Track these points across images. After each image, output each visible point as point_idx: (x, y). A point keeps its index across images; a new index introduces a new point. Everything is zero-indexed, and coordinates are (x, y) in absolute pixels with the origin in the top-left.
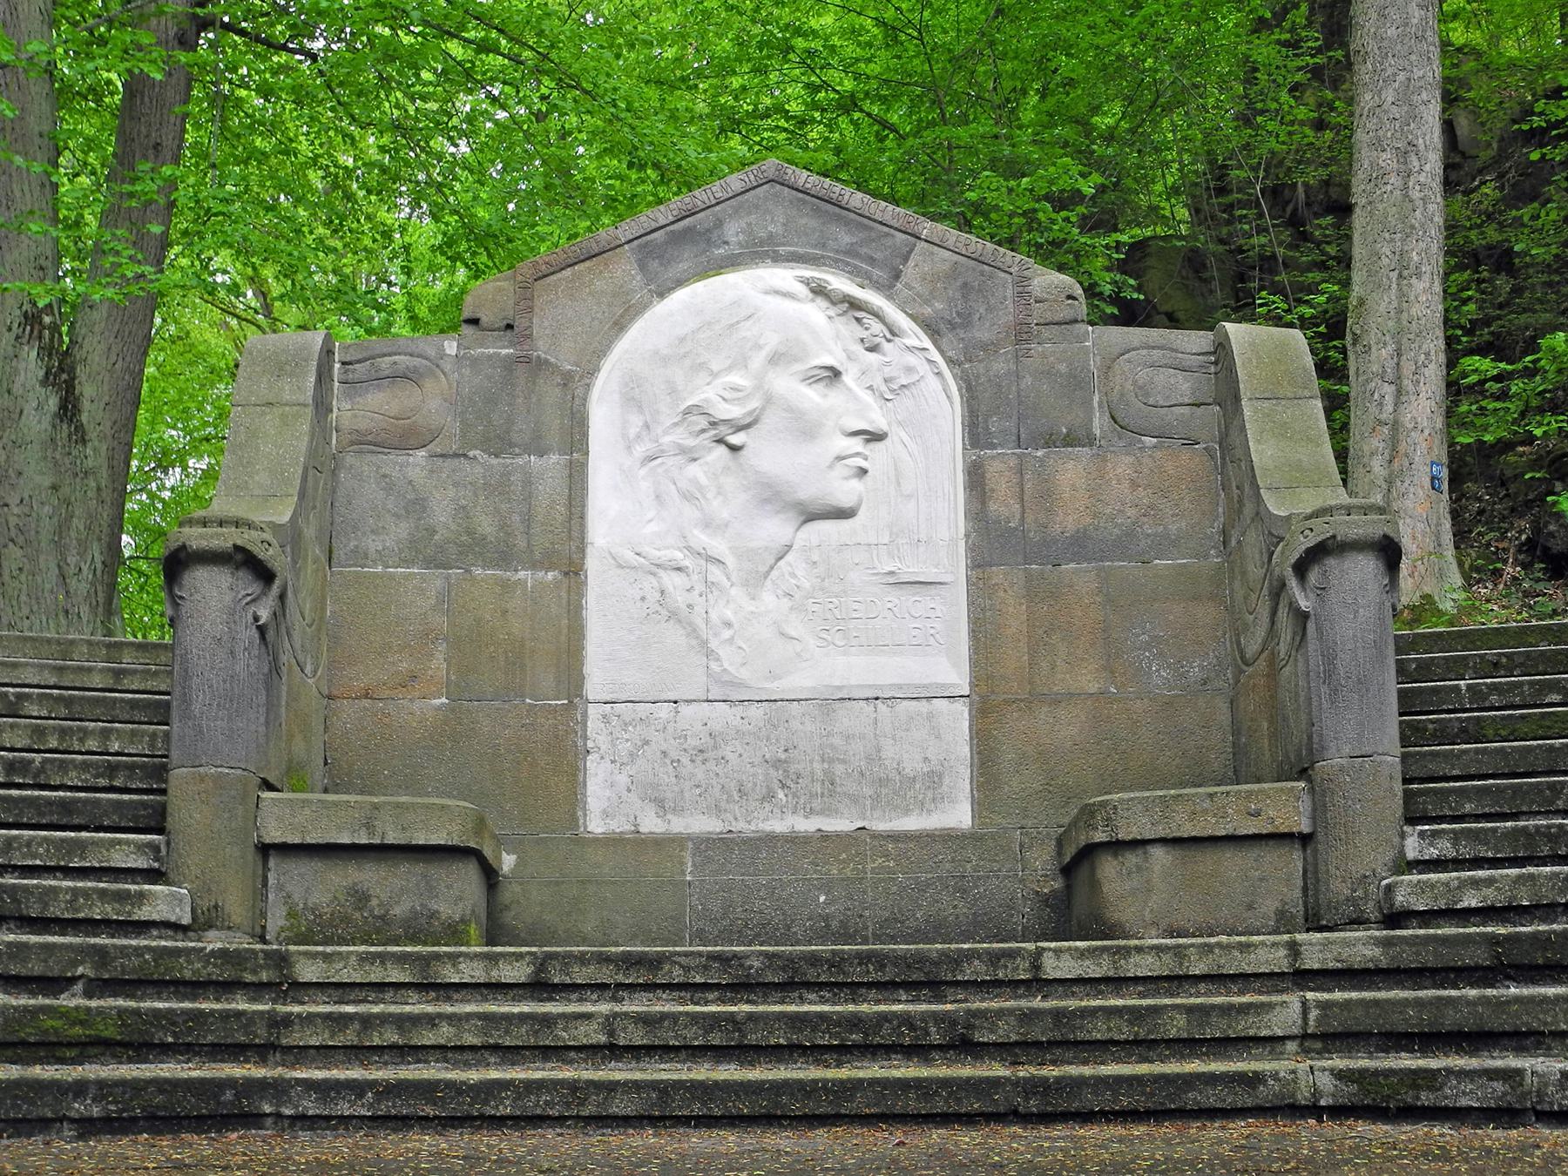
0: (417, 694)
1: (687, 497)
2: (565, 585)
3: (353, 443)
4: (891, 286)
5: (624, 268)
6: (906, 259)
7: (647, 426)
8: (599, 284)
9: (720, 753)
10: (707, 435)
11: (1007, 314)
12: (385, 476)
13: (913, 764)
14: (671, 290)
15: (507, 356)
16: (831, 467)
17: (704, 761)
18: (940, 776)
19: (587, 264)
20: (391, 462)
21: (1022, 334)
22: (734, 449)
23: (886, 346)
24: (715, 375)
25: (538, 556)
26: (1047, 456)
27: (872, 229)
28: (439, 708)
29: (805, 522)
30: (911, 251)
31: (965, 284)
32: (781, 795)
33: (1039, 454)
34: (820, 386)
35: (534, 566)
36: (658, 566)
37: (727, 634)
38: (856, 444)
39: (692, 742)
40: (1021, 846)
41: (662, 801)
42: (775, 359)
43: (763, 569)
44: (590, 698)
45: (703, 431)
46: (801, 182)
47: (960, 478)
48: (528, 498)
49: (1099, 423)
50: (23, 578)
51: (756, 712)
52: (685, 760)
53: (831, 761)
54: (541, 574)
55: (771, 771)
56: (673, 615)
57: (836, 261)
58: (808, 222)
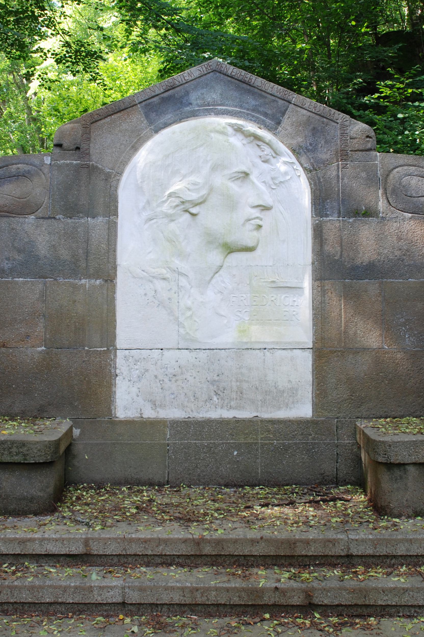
0: (29, 345)
4: (276, 129)
6: (283, 114)
7: (148, 202)
8: (125, 126)
9: (185, 377)
10: (177, 208)
12: (13, 229)
13: (282, 383)
15: (77, 164)
16: (244, 225)
17: (176, 381)
18: (297, 390)
19: (119, 115)
22: (193, 215)
23: (273, 160)
24: (184, 176)
25: (91, 271)
26: (354, 221)
27: (266, 97)
28: (40, 352)
29: (229, 253)
30: (287, 109)
31: (314, 128)
32: (215, 398)
33: (351, 220)
34: (238, 182)
35: (89, 277)
36: (154, 277)
37: (189, 313)
38: (256, 213)
39: (170, 371)
40: (337, 427)
41: (155, 401)
42: (215, 168)
43: (208, 278)
44: (118, 347)
46: (229, 72)
47: (310, 233)
48: (87, 241)
51: (203, 355)
52: (166, 380)
53: (241, 381)
54: (93, 281)
55: (212, 387)
56: (161, 304)
57: (248, 114)
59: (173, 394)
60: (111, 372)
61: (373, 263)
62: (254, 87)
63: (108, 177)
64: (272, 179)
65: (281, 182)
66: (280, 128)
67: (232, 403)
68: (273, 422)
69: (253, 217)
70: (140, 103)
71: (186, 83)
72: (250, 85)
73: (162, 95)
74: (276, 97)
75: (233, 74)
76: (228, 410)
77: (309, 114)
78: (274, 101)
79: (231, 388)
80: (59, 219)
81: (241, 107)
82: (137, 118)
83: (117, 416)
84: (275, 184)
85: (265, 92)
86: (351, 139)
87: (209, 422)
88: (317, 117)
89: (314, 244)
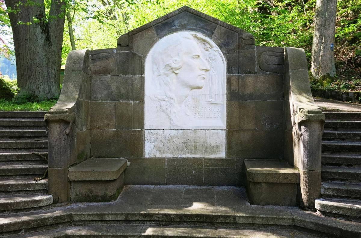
1: (166, 84)
2: (140, 104)
3: (94, 73)
5: (153, 32)
6: (215, 29)
9: (173, 141)
10: (170, 71)
11: (237, 43)
13: (213, 144)
14: (163, 37)
15: (127, 53)
18: (219, 146)
20: (103, 77)
21: (240, 47)
22: (176, 74)
26: (245, 76)
28: (114, 131)
29: (192, 89)
30: (216, 27)
31: (228, 36)
32: (185, 149)
33: (243, 75)
35: (133, 100)
36: (160, 100)
38: (203, 72)
40: (236, 162)
41: (161, 151)
44: (146, 129)
45: (170, 70)
47: (225, 81)
49: (256, 68)
50: (40, 74)
51: (180, 132)
52: (165, 142)
53: (196, 143)
54: (135, 101)
55: (184, 145)
56: (163, 111)
58: (192, 20)
59: (168, 148)
60: (143, 139)
61: (252, 94)
62: (202, 18)
63: (140, 57)
64: (210, 58)
65: (213, 59)
66: (213, 36)
67: (193, 152)
68: (209, 159)
69: (202, 74)
70: (154, 25)
71: (173, 16)
72: (200, 17)
73: (162, 22)
74: (211, 22)
75: (193, 12)
76: (191, 154)
77: (226, 29)
78: (211, 24)
79: (192, 145)
80: (121, 76)
81: (196, 26)
82: (153, 32)
83: (146, 156)
84: (211, 60)
85: (207, 20)
86: (244, 40)
87: (183, 159)
88: (229, 30)
89: (227, 86)
